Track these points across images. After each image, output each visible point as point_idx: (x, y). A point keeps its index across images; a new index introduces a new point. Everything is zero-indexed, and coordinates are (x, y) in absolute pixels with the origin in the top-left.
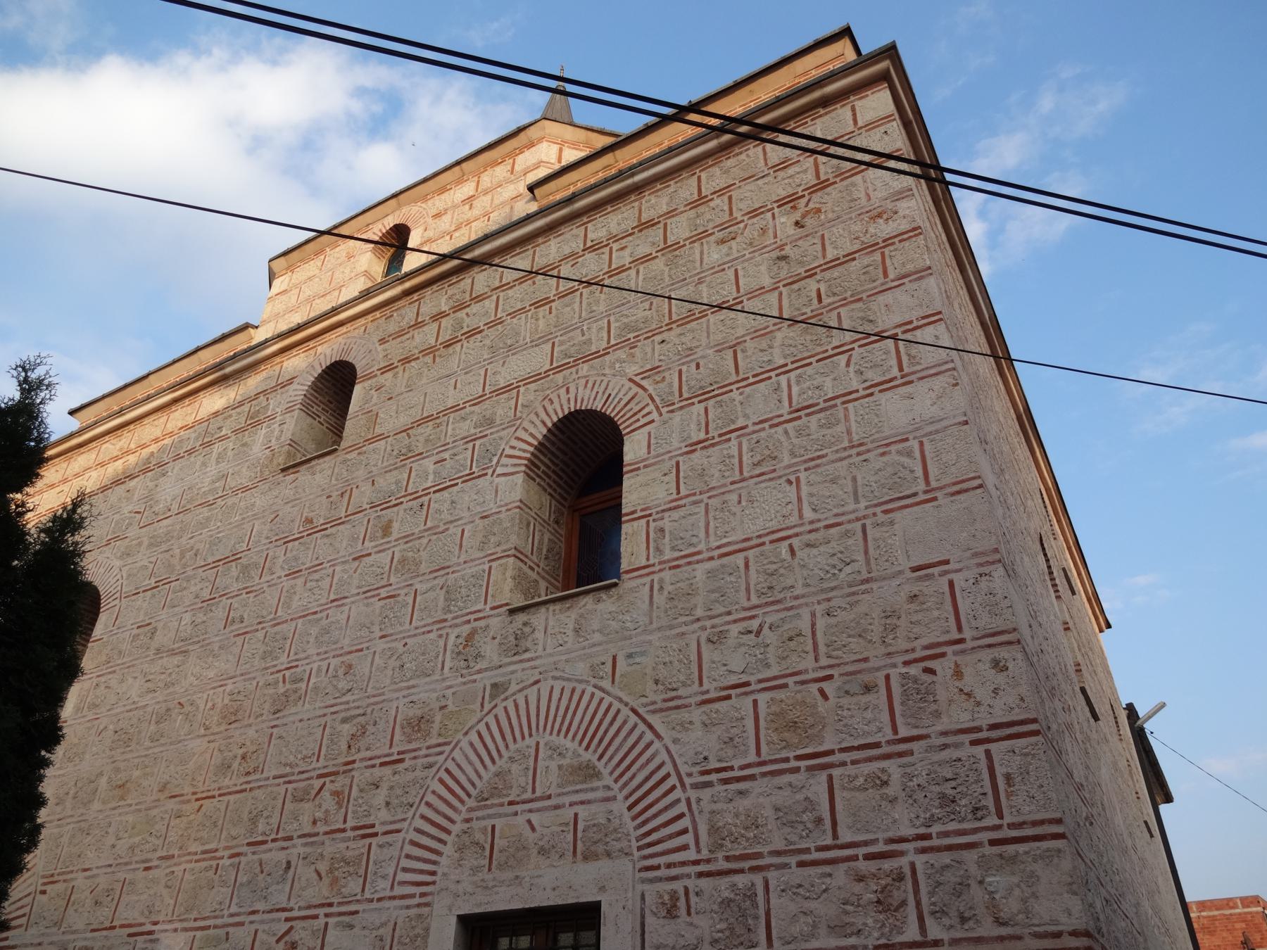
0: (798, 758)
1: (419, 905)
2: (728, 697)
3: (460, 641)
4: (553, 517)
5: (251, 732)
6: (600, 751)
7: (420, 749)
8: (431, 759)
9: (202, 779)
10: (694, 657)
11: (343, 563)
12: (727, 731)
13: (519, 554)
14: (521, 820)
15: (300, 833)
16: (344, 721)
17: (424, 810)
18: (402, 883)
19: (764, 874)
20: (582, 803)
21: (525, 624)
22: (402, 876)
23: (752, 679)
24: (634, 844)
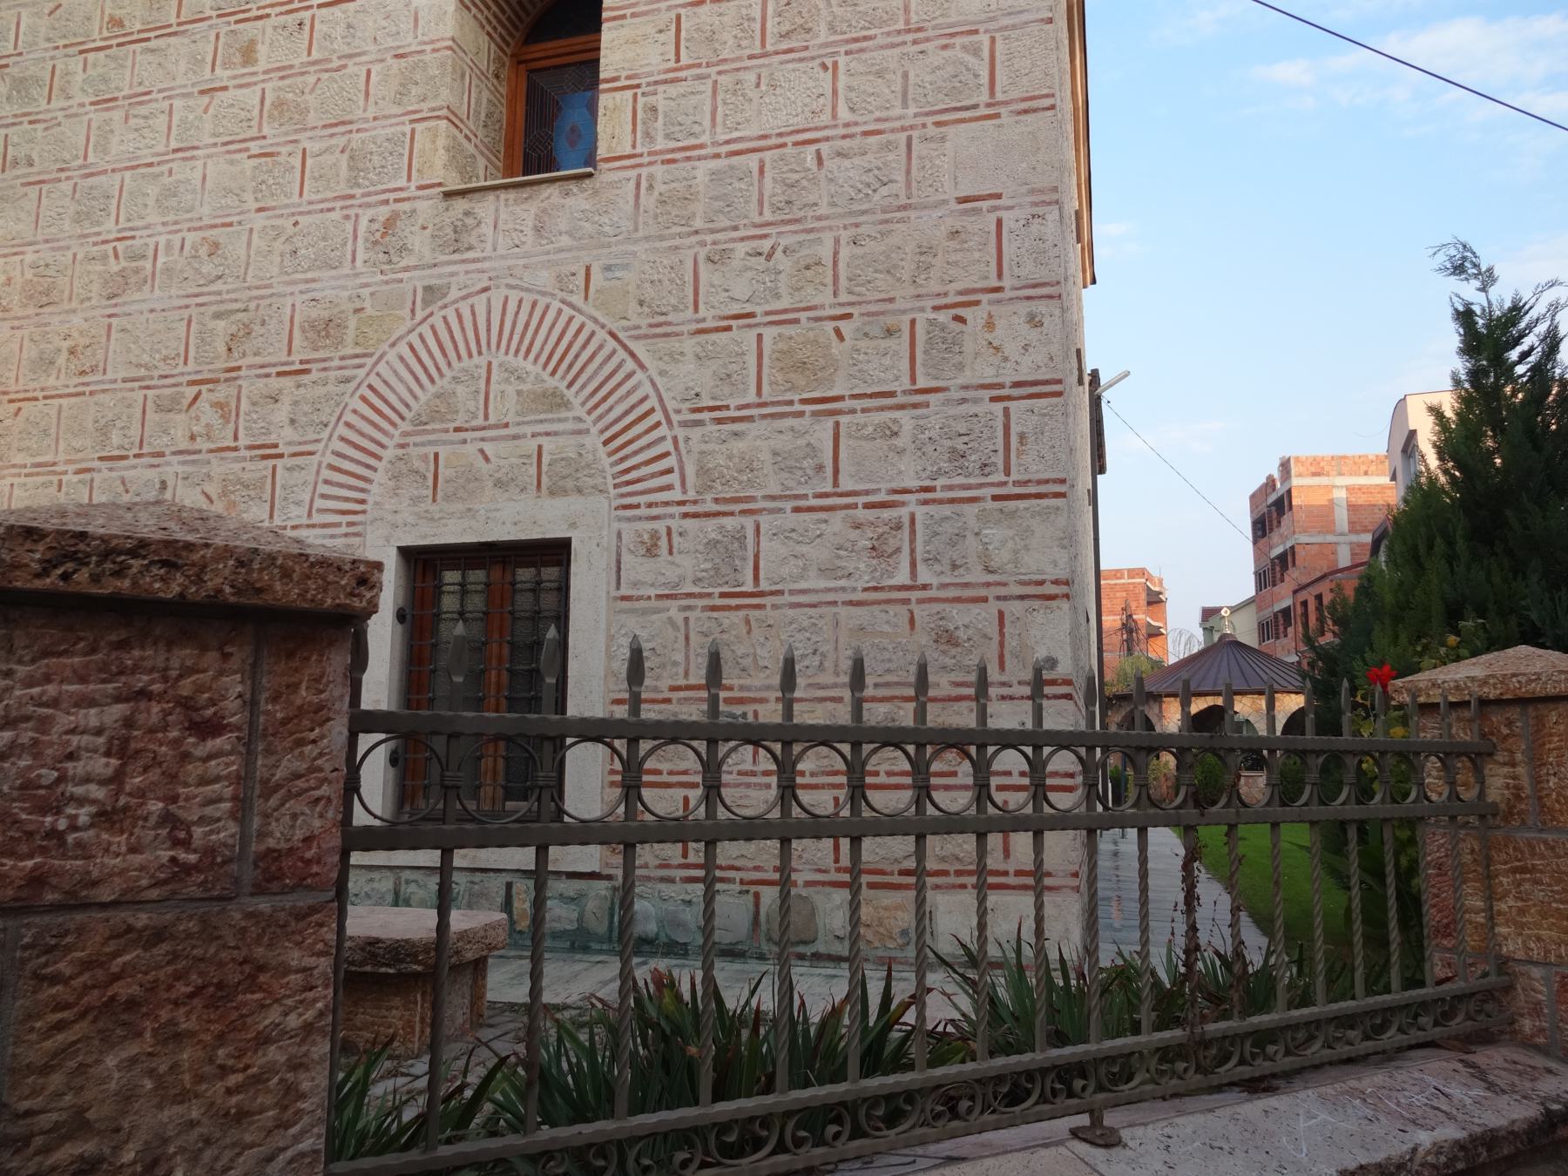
0: (804, 401)
1: (346, 535)
2: (729, 328)
3: (375, 226)
4: (492, 68)
5: (77, 320)
6: (570, 377)
7: (331, 359)
8: (347, 373)
9: (13, 375)
10: (689, 278)
11: (184, 95)
12: (724, 366)
13: (453, 118)
14: (471, 449)
15: (174, 449)
16: (218, 316)
17: (342, 430)
18: (320, 511)
19: (755, 517)
20: (548, 434)
21: (467, 214)
22: (320, 503)
23: (758, 310)
24: (611, 482)
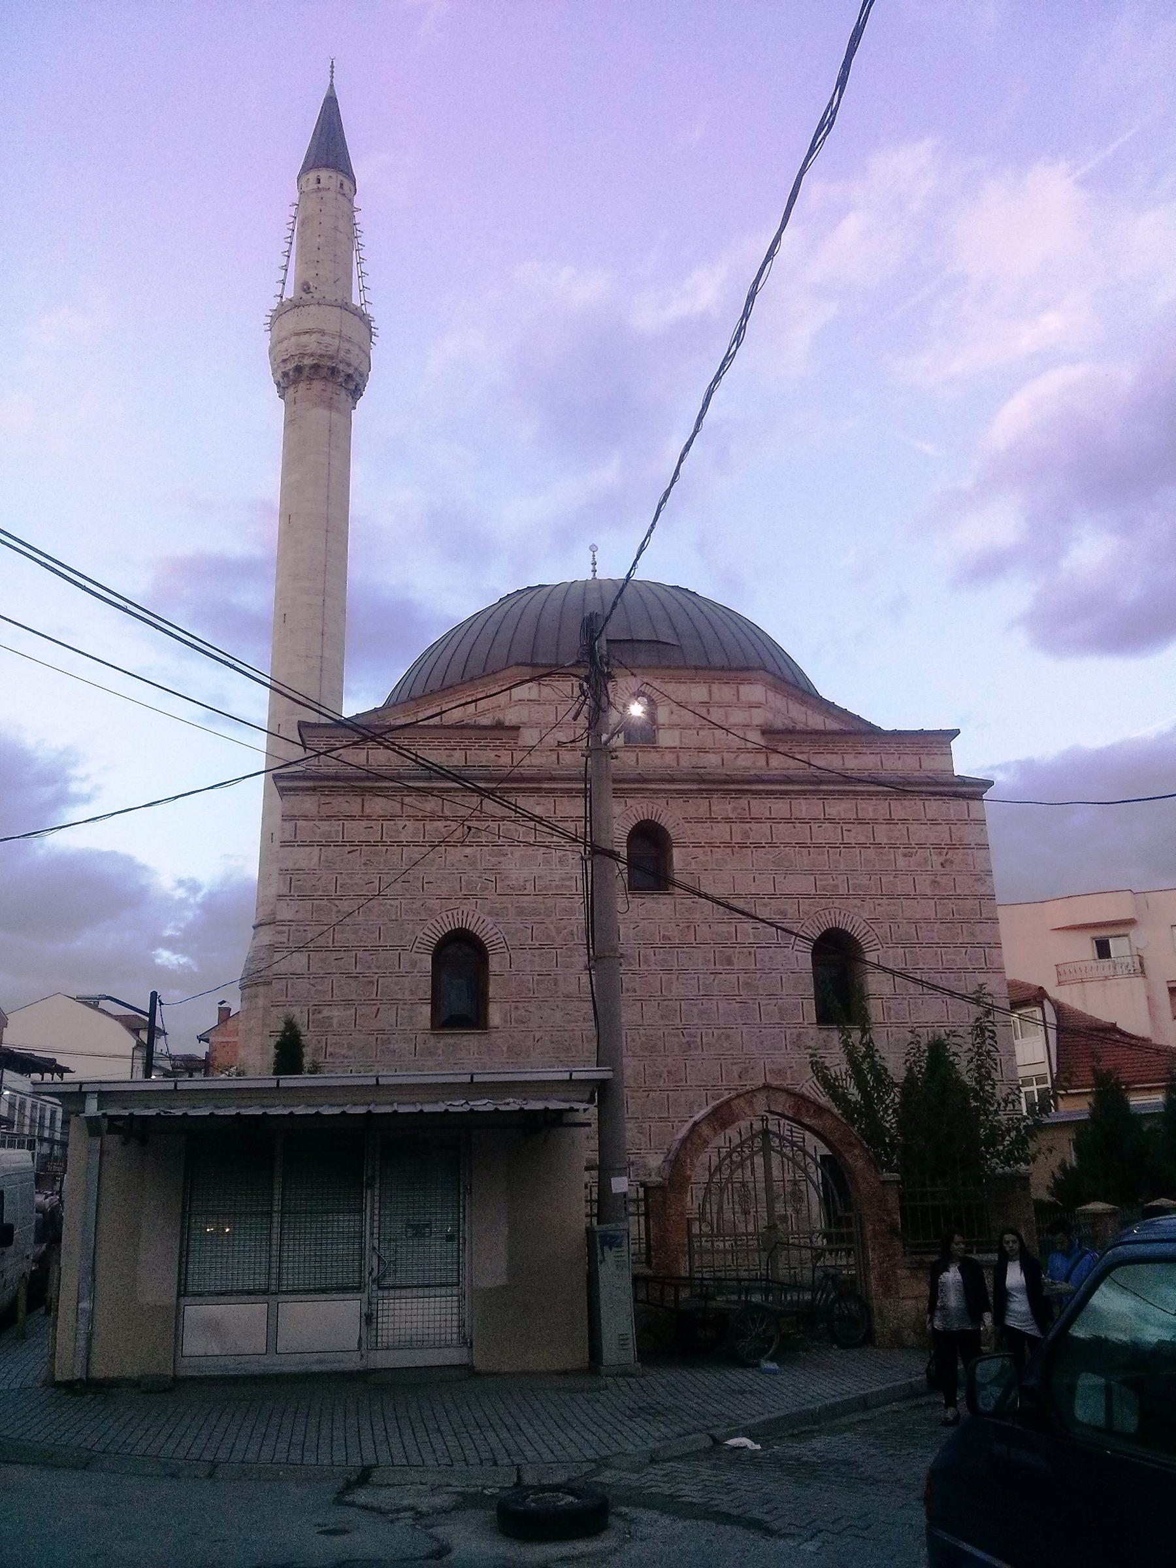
5: (670, 1060)
16: (733, 1064)
